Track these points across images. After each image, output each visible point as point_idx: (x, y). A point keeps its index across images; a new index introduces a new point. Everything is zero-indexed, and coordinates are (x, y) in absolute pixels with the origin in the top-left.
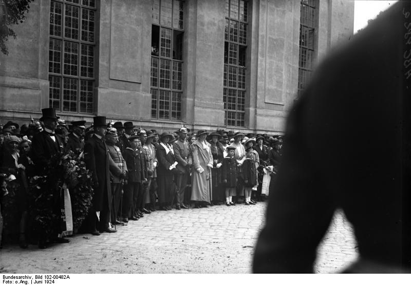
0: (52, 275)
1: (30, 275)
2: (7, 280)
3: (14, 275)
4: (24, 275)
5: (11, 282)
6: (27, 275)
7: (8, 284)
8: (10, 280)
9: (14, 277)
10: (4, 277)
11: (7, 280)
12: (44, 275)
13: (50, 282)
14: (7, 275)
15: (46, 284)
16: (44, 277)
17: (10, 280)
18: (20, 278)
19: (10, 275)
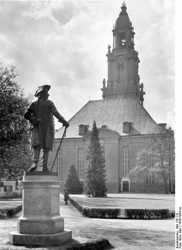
2: (179, 246)
3: (176, 241)
4: (176, 236)
8: (179, 244)
9: (177, 241)
10: (177, 248)
11: (179, 246)
13: (180, 221)
16: (177, 224)
17: (179, 244)
18: (178, 238)
19: (176, 244)
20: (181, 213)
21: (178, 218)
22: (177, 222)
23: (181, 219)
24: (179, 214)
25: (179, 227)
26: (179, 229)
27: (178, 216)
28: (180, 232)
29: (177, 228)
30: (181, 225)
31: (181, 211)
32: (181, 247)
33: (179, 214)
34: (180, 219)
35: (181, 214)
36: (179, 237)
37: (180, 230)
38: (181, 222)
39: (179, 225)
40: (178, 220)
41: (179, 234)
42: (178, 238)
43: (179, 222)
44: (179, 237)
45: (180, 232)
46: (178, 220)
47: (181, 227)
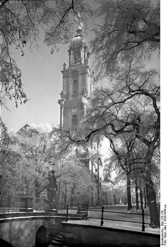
0: (161, 215)
1: (161, 229)
2: (164, 243)
5: (165, 240)
6: (161, 231)
7: (166, 242)
8: (164, 241)
9: (162, 238)
10: (162, 245)
12: (161, 221)
13: (165, 219)
14: (161, 243)
15: (166, 221)
16: (162, 221)
17: (164, 241)
18: (163, 235)
19: (161, 241)
21: (164, 216)
22: (162, 219)
24: (164, 212)
25: (164, 225)
26: (164, 226)
27: (164, 214)
28: (165, 229)
29: (162, 225)
33: (164, 212)
36: (164, 234)
37: (165, 228)
39: (164, 222)
40: (164, 218)
41: (164, 231)
42: (163, 235)
43: (164, 219)
44: (164, 234)
45: (165, 229)
46: (164, 218)
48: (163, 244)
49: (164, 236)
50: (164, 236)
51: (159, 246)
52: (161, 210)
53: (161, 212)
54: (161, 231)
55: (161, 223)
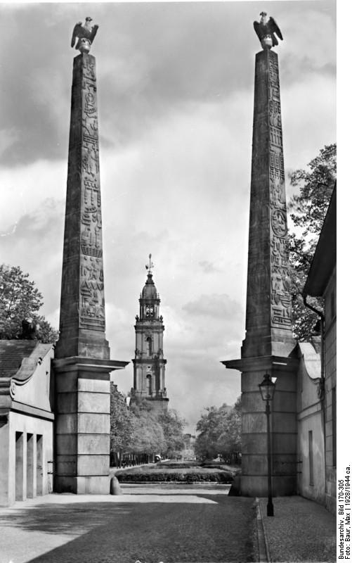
0: (338, 491)
1: (338, 522)
2: (345, 553)
5: (348, 548)
8: (345, 549)
9: (342, 543)
10: (341, 558)
12: (338, 503)
13: (347, 499)
14: (338, 554)
16: (342, 503)
17: (345, 549)
19: (338, 549)
20: (351, 479)
21: (344, 492)
22: (341, 499)
23: (351, 493)
24: (345, 483)
25: (345, 512)
26: (345, 516)
28: (346, 522)
29: (342, 513)
30: (350, 506)
31: (351, 475)
32: (350, 556)
33: (345, 483)
34: (347, 494)
35: (350, 482)
36: (345, 533)
37: (348, 519)
38: (351, 500)
39: (345, 506)
40: (344, 496)
42: (342, 536)
43: (344, 499)
44: (345, 533)
45: (346, 522)
46: (344, 496)
47: (350, 512)
48: (344, 556)
49: (344, 539)
50: (344, 539)
51: (332, 554)
52: (339, 478)
53: (338, 483)
54: (338, 526)
55: (338, 507)
